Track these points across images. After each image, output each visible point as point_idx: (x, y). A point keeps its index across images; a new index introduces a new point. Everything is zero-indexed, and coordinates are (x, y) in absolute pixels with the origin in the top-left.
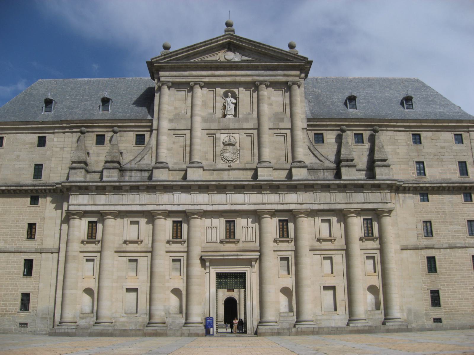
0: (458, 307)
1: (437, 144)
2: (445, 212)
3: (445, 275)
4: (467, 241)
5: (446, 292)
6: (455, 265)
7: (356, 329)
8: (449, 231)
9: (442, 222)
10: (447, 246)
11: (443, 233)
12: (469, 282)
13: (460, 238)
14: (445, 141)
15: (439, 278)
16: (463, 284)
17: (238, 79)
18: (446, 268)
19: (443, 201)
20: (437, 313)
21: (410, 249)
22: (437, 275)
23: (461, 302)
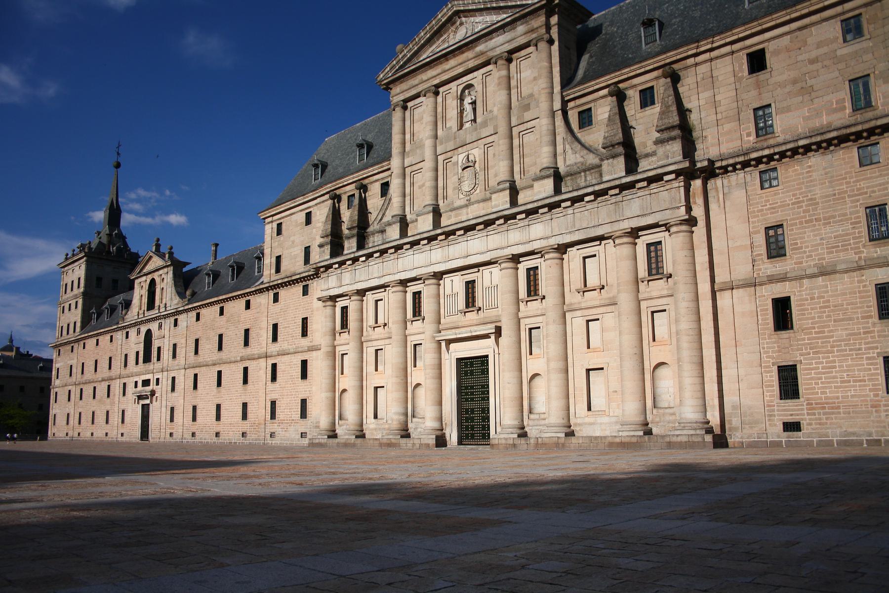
0: (838, 398)
1: (800, 58)
2: (815, 199)
3: (811, 333)
4: (863, 255)
5: (812, 369)
6: (833, 311)
7: (618, 440)
8: (821, 239)
9: (806, 222)
10: (816, 270)
11: (807, 245)
12: (866, 343)
13: (847, 250)
14: (819, 45)
15: (798, 340)
16: (851, 350)
17: (471, 64)
18: (814, 318)
19: (810, 176)
20: (791, 410)
21: (738, 287)
22: (792, 335)
23: (846, 387)
